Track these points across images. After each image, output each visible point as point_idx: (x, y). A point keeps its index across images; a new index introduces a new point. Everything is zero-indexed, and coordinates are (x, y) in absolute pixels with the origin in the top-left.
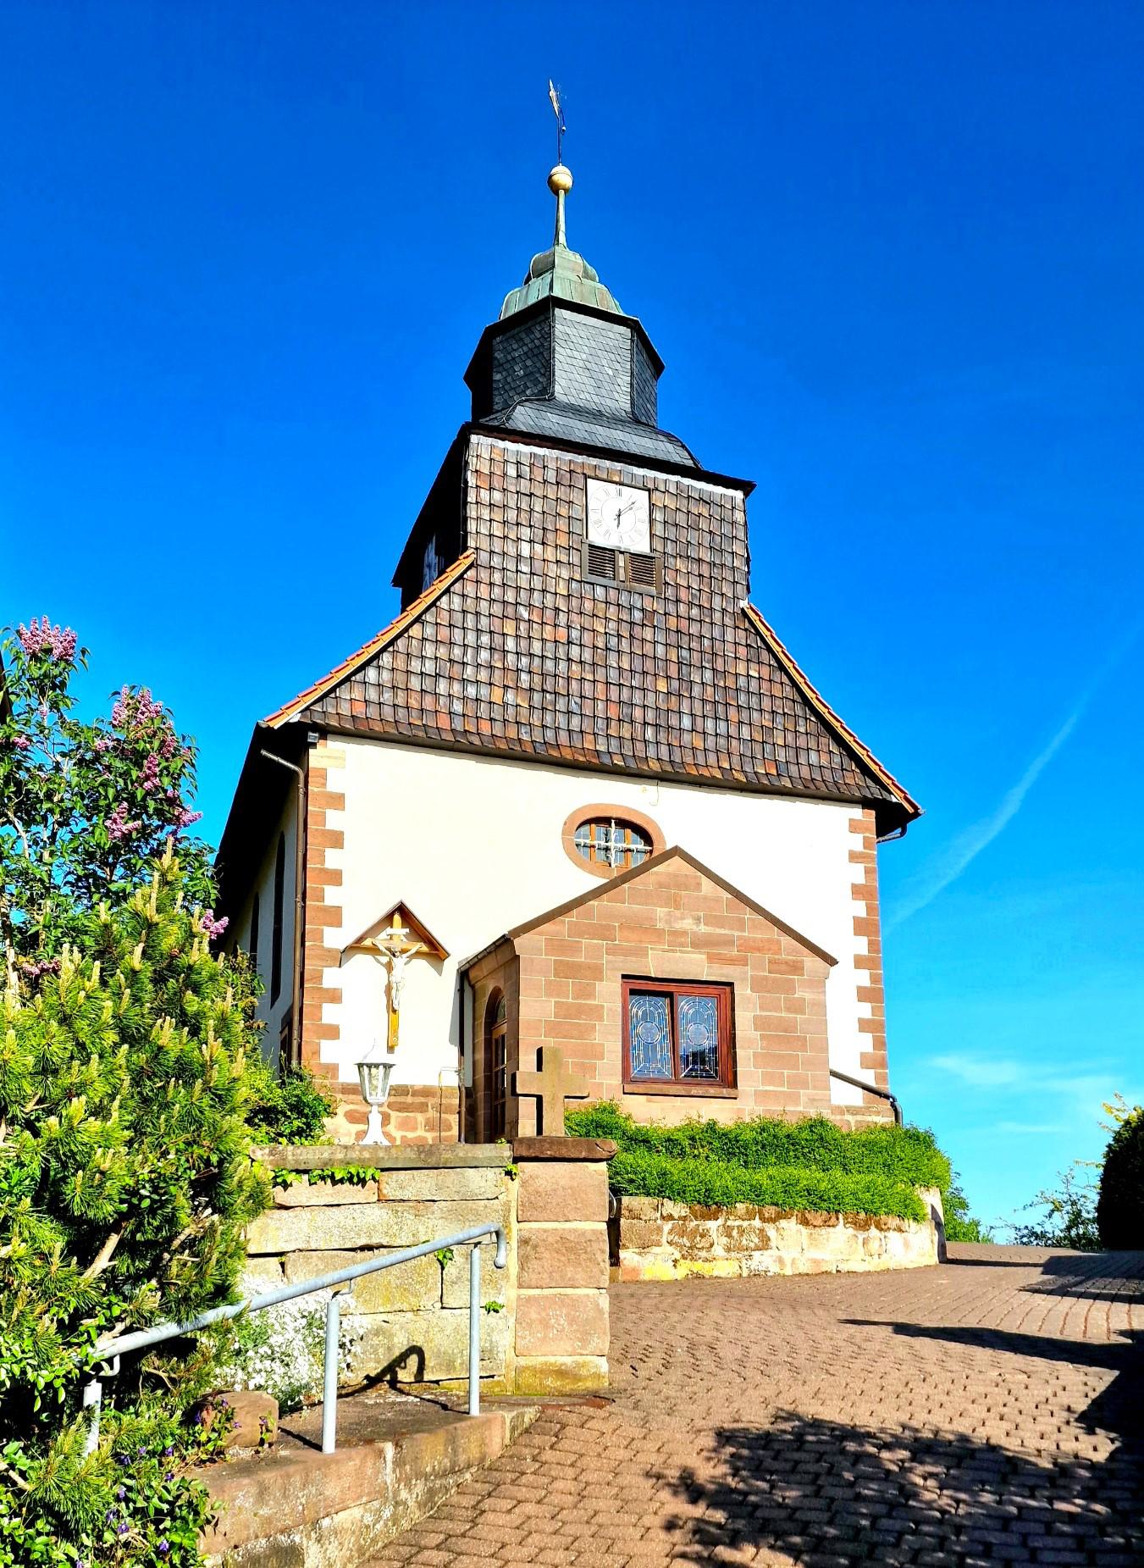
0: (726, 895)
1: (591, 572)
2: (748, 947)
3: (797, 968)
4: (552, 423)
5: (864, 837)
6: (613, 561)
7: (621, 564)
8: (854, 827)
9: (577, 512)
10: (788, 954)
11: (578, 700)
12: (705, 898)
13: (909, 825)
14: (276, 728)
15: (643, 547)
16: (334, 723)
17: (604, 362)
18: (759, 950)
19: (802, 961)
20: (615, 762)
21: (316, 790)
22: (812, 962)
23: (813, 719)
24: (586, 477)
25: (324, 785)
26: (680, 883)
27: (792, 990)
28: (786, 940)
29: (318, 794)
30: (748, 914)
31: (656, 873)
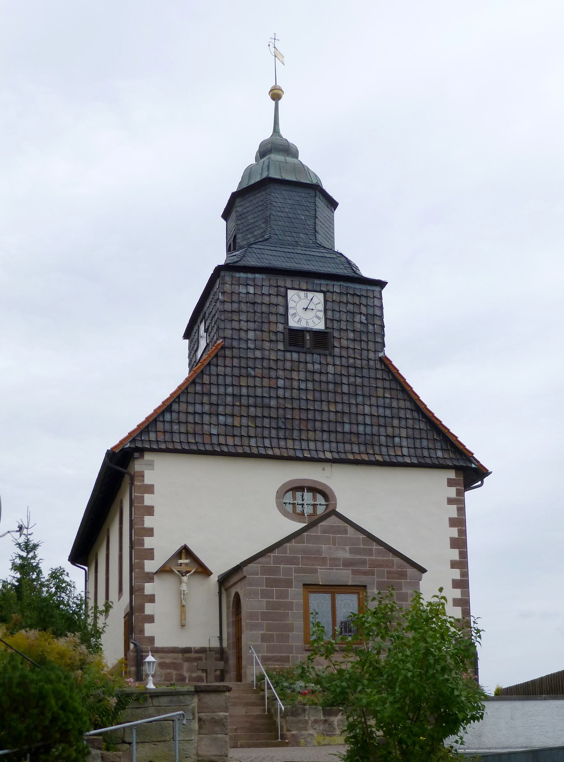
0: (362, 536)
1: (290, 345)
2: (374, 564)
3: (403, 575)
4: (91, 596)
5: (457, 489)
6: (303, 337)
7: (308, 338)
8: (451, 483)
9: (281, 310)
10: (398, 568)
11: (283, 420)
12: (350, 538)
13: (485, 480)
14: (117, 452)
15: (320, 326)
16: (147, 446)
17: (299, 212)
18: (381, 566)
19: (406, 572)
20: (305, 455)
21: (139, 484)
22: (411, 571)
23: (423, 420)
24: (287, 289)
25: (143, 481)
26: (337, 531)
27: (400, 588)
28: (396, 560)
29: (139, 486)
30: (375, 547)
31: (321, 526)
